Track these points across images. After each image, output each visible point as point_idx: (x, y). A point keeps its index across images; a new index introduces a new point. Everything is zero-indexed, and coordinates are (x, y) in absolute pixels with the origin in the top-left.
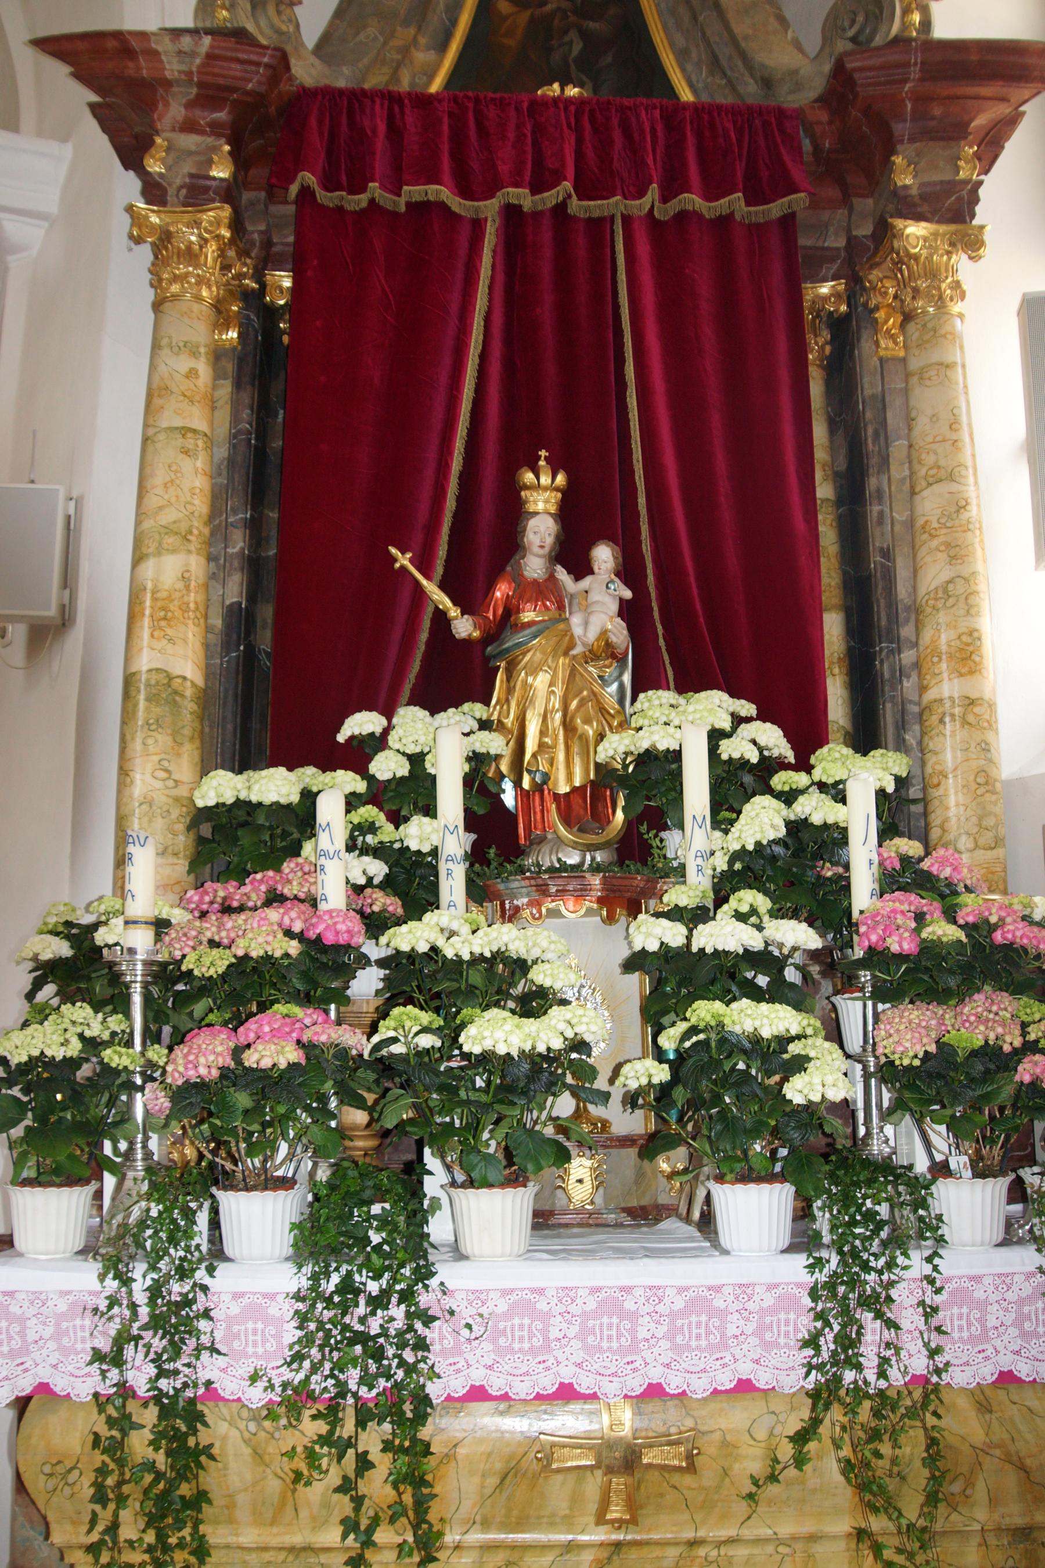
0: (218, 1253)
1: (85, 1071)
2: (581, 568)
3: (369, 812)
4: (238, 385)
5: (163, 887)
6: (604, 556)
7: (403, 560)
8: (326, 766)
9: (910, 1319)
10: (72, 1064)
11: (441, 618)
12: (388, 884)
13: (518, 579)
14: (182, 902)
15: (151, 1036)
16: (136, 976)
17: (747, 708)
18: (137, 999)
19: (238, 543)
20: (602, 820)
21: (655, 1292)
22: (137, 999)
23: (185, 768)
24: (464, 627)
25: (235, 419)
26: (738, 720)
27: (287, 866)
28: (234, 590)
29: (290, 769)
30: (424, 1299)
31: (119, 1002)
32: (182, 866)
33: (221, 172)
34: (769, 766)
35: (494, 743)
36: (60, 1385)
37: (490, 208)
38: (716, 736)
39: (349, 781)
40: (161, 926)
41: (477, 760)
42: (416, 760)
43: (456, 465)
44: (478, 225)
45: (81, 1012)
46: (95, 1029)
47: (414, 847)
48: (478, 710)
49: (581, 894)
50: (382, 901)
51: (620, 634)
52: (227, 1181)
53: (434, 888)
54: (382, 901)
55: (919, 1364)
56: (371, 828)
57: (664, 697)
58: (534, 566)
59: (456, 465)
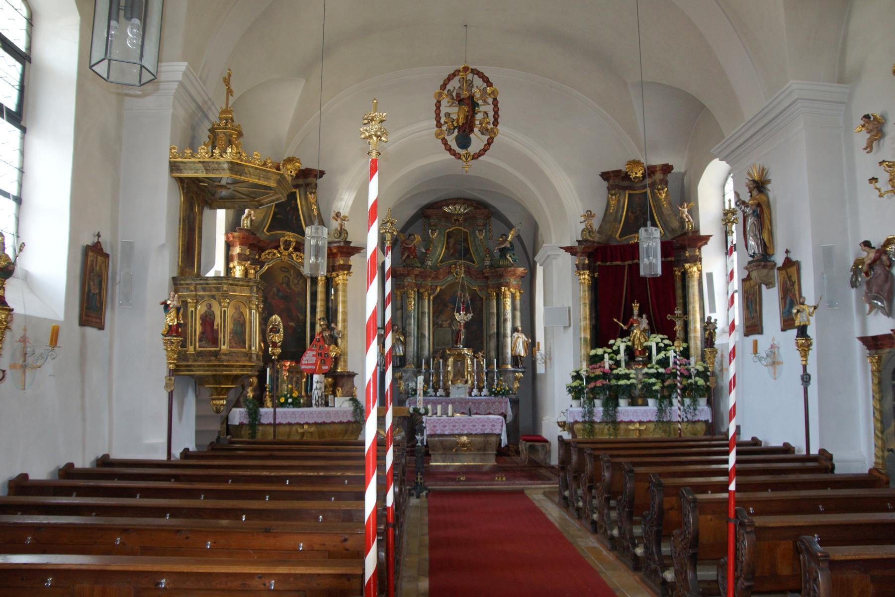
0: (594, 406)
1: (580, 387)
2: (642, 318)
3: (612, 355)
4: (592, 291)
5: (587, 365)
6: (644, 316)
7: (615, 320)
8: (608, 348)
9: (668, 414)
10: (578, 387)
11: (622, 327)
12: (615, 364)
13: (633, 319)
14: (588, 367)
15: (586, 384)
16: (584, 377)
17: (666, 337)
18: (584, 380)
19: (594, 315)
20: (645, 354)
21: (640, 410)
22: (584, 380)
23: (589, 349)
24: (625, 328)
25: (592, 296)
26: (664, 339)
27: (602, 362)
28: (594, 322)
29: (602, 348)
30: (616, 410)
31: (583, 380)
32: (588, 362)
33: (587, 262)
34: (666, 346)
35: (630, 344)
36: (578, 420)
37: (627, 263)
38: (657, 344)
39: (609, 350)
40: (587, 371)
41: (627, 347)
42: (619, 347)
43: (623, 303)
44: (624, 266)
45: (578, 381)
46: (580, 383)
47: (618, 359)
48: (628, 338)
49: (640, 365)
50: (614, 367)
51: (647, 327)
52: (596, 398)
53: (620, 364)
54: (614, 367)
55: (669, 418)
56: (612, 357)
57: (654, 335)
58: (635, 318)
59: (623, 303)
